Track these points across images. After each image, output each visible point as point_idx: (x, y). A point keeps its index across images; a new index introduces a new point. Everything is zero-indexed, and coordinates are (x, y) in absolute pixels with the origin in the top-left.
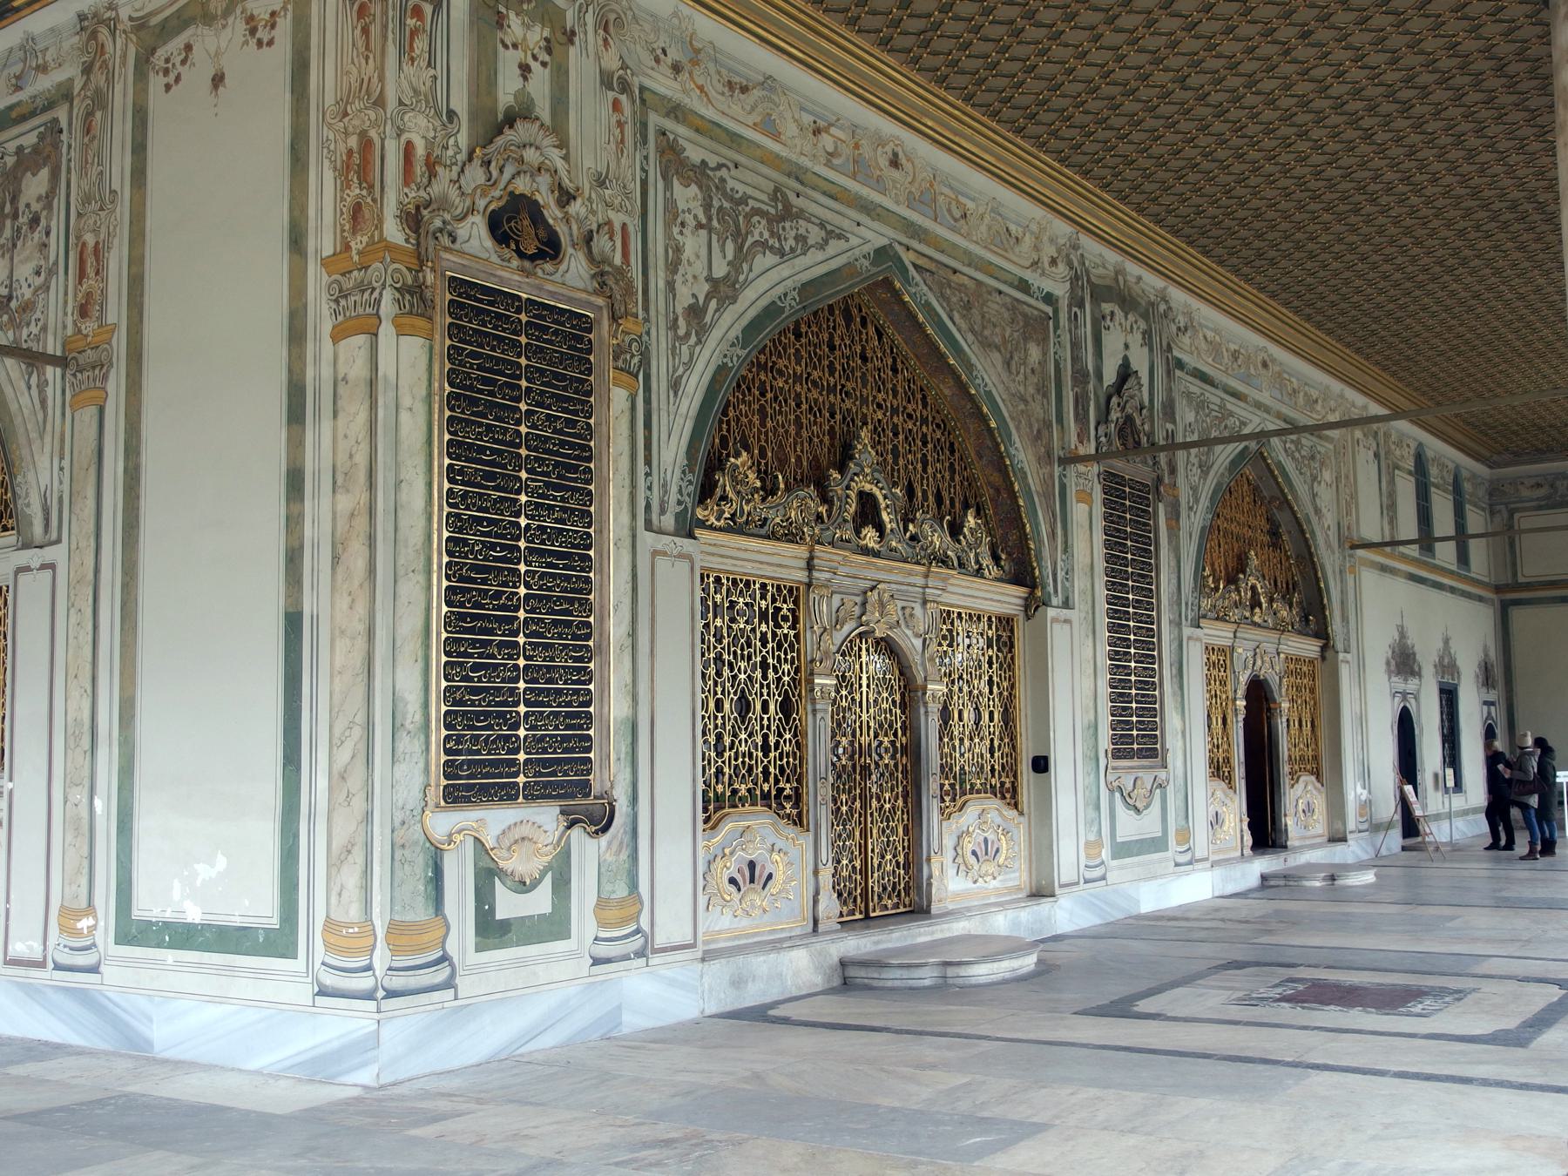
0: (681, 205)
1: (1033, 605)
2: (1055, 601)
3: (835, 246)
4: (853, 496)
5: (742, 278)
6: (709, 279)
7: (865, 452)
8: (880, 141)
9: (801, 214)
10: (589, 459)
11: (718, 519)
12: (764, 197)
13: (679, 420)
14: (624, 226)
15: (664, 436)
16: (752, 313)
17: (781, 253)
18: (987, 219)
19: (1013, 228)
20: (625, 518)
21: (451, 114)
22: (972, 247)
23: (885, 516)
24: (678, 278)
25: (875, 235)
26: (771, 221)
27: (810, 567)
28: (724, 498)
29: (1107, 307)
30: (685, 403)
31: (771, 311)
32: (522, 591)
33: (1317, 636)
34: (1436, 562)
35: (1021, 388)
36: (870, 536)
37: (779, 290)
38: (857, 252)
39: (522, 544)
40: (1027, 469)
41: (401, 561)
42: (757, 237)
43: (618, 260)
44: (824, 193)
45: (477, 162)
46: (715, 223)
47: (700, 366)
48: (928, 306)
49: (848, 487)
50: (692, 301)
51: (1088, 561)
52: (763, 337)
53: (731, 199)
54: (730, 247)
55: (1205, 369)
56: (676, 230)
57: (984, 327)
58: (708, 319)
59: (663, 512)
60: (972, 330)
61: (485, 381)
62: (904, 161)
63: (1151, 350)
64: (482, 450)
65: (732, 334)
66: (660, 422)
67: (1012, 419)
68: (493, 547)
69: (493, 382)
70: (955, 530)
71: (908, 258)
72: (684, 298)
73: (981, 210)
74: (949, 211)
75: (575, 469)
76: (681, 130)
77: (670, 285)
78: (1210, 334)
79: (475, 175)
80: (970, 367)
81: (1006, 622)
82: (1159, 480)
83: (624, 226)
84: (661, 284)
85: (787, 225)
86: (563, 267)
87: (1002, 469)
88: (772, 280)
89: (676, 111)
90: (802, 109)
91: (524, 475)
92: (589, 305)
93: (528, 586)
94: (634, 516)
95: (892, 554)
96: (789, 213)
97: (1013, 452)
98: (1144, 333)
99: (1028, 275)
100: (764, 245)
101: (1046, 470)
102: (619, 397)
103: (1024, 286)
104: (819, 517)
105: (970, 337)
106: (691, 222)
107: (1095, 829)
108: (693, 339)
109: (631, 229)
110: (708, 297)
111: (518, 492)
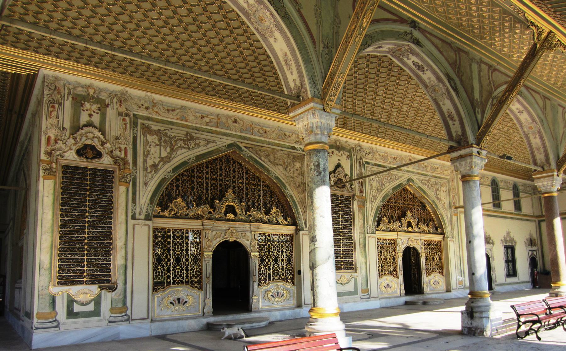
0: (150, 141)
1: (297, 231)
2: (305, 229)
3: (210, 145)
4: (224, 206)
5: (173, 156)
6: (160, 157)
7: (230, 194)
8: (228, 117)
9: (197, 138)
10: (112, 204)
11: (169, 215)
12: (183, 136)
13: (147, 193)
14: (125, 148)
15: (141, 196)
16: (177, 164)
17: (189, 149)
18: (276, 132)
19: (286, 133)
20: (123, 217)
22: (268, 140)
23: (237, 210)
24: (148, 158)
25: (228, 141)
26: (184, 141)
27: (203, 225)
28: (172, 210)
30: (149, 189)
31: (184, 163)
32: (86, 236)
33: (441, 234)
34: (503, 210)
35: (292, 175)
36: (230, 216)
37: (188, 158)
38: (220, 146)
39: (87, 225)
40: (293, 195)
41: (43, 231)
42: (179, 145)
43: (123, 156)
44: (207, 132)
45: (71, 139)
46: (163, 144)
47: (156, 178)
49: (222, 204)
50: (153, 163)
52: (182, 171)
53: (169, 137)
54: (168, 149)
55: (380, 163)
56: (148, 147)
57: (275, 160)
58: (159, 167)
59: (140, 214)
60: (270, 161)
61: (74, 188)
62: (239, 121)
63: (351, 160)
64: (73, 204)
65: (168, 170)
66: (139, 194)
67: (287, 183)
68: (76, 226)
69: (78, 188)
70: (267, 213)
71: (241, 145)
72: (150, 162)
73: (273, 130)
74: (258, 132)
75: (106, 206)
76: (151, 123)
77: (145, 161)
78: (381, 154)
79: (71, 141)
80: (268, 170)
81: (291, 236)
82: (354, 195)
83: (125, 148)
84: (142, 160)
85: (191, 142)
86: (102, 160)
87: (285, 196)
88: (183, 155)
90: (196, 112)
91: (87, 209)
92: (112, 168)
93: (88, 234)
94: (127, 216)
96: (192, 138)
97: (287, 191)
98: (348, 157)
99: (294, 145)
100: (182, 148)
101: (302, 195)
102: (122, 189)
103: (294, 148)
104: (210, 213)
105: (269, 163)
106: (153, 144)
108: (153, 172)
109: (128, 149)
110: (159, 162)
111: (86, 213)
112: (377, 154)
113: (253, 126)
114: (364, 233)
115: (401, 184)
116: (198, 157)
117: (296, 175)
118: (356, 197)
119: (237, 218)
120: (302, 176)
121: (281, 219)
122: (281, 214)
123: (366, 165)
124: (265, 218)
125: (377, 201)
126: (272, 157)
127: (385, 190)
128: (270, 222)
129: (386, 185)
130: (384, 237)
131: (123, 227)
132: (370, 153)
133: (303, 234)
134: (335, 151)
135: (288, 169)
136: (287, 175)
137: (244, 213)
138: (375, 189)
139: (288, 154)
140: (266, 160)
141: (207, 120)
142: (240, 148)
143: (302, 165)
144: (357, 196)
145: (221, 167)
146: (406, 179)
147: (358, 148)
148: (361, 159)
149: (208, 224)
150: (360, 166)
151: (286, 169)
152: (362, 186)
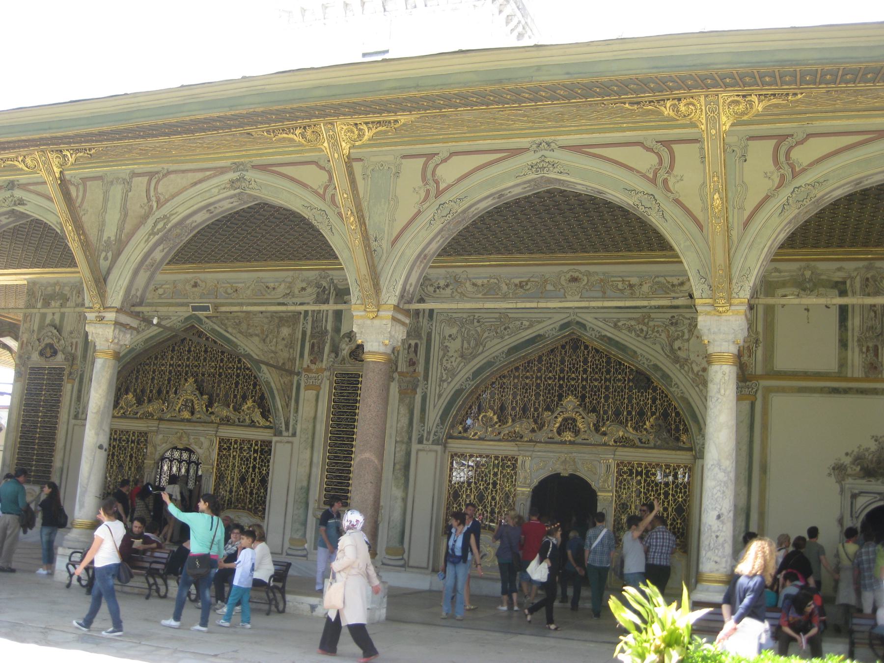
2: (285, 434)
8: (187, 281)
20: (66, 416)
21: (33, 331)
22: (239, 301)
23: (196, 407)
28: (122, 408)
35: (273, 348)
40: (271, 380)
48: (213, 330)
51: (312, 414)
57: (248, 329)
74: (226, 292)
95: (200, 422)
99: (281, 300)
101: (286, 379)
105: (238, 335)
107: (300, 533)
112: (468, 284)
113: (219, 286)
115: (539, 336)
116: (147, 341)
117: (281, 347)
118: (396, 375)
119: (194, 418)
120: (290, 348)
121: (258, 417)
122: (258, 411)
124: (233, 416)
125: (457, 379)
126: (244, 326)
127: (486, 354)
128: (241, 423)
131: (65, 427)
132: (447, 286)
133: (276, 442)
135: (268, 340)
136: (266, 349)
137: (205, 409)
138: (456, 355)
139: (272, 317)
140: (234, 331)
141: (161, 291)
142: (200, 320)
143: (294, 330)
144: (401, 374)
145: (190, 348)
146: (557, 326)
149: (152, 425)
151: (264, 340)
152: (416, 352)
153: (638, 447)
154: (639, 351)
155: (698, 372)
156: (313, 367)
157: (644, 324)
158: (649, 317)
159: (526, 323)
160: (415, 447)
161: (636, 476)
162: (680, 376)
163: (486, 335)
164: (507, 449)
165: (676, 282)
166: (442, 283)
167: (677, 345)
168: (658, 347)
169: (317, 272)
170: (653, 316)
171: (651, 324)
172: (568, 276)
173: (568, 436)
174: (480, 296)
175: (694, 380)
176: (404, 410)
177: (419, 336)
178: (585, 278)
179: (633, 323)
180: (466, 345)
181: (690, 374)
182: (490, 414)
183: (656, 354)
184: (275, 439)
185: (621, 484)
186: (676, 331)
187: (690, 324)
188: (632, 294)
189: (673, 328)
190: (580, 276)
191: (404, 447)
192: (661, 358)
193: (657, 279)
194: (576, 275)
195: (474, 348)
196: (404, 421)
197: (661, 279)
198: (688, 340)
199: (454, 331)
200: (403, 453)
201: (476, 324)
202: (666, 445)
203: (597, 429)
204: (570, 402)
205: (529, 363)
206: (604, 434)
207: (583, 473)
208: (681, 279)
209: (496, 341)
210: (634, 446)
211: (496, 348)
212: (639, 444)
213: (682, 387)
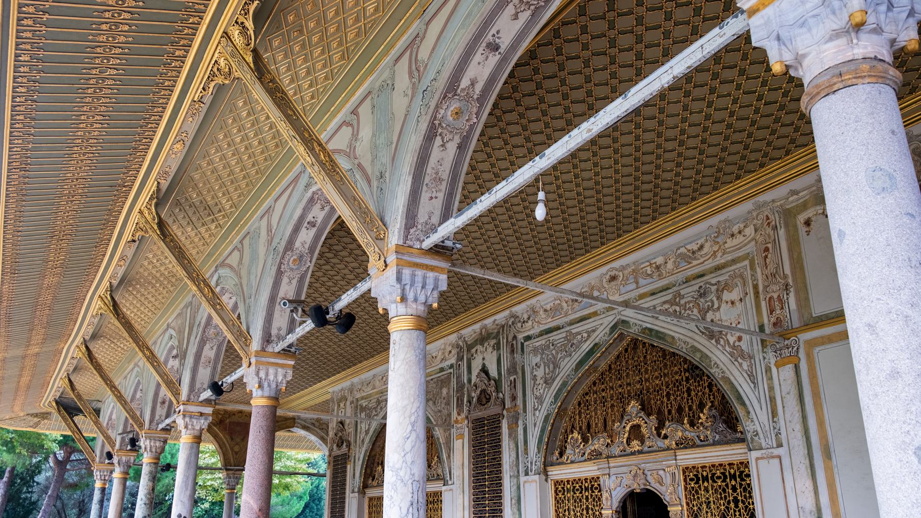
29: (473, 350)
89: (362, 398)
99: (440, 366)
103: (442, 370)
112: (542, 312)
114: (518, 476)
115: (596, 344)
123: (526, 344)
125: (544, 405)
127: (561, 375)
129: (562, 364)
130: (577, 476)
132: (529, 318)
134: (479, 347)
138: (542, 382)
147: (510, 323)
148: (515, 337)
150: (512, 352)
153: (698, 446)
154: (676, 336)
155: (734, 342)
156: (459, 418)
157: (677, 305)
158: (680, 294)
159: (585, 335)
160: (523, 479)
161: (703, 482)
162: (718, 353)
163: (559, 356)
164: (587, 470)
165: (695, 248)
166: (526, 316)
167: (710, 316)
168: (692, 326)
169: (455, 335)
170: (682, 292)
171: (682, 302)
172: (608, 277)
173: (636, 445)
174: (550, 320)
175: (732, 354)
176: (512, 446)
177: (516, 373)
178: (621, 274)
179: (666, 306)
180: (547, 370)
181: (727, 348)
182: (576, 435)
183: (690, 334)
184: (444, 488)
185: (692, 494)
186: (706, 302)
187: (717, 290)
188: (659, 275)
189: (702, 300)
190: (617, 273)
191: (515, 480)
192: (697, 338)
193: (679, 252)
194: (613, 273)
195: (553, 372)
196: (514, 455)
197: (683, 250)
198: (719, 308)
199: (538, 359)
200: (515, 487)
201: (552, 347)
202: (725, 439)
203: (659, 435)
204: (633, 407)
205: (602, 374)
206: (666, 437)
207: (655, 486)
208: (700, 242)
209: (567, 359)
210: (694, 446)
211: (568, 365)
212: (698, 442)
213: (721, 365)
